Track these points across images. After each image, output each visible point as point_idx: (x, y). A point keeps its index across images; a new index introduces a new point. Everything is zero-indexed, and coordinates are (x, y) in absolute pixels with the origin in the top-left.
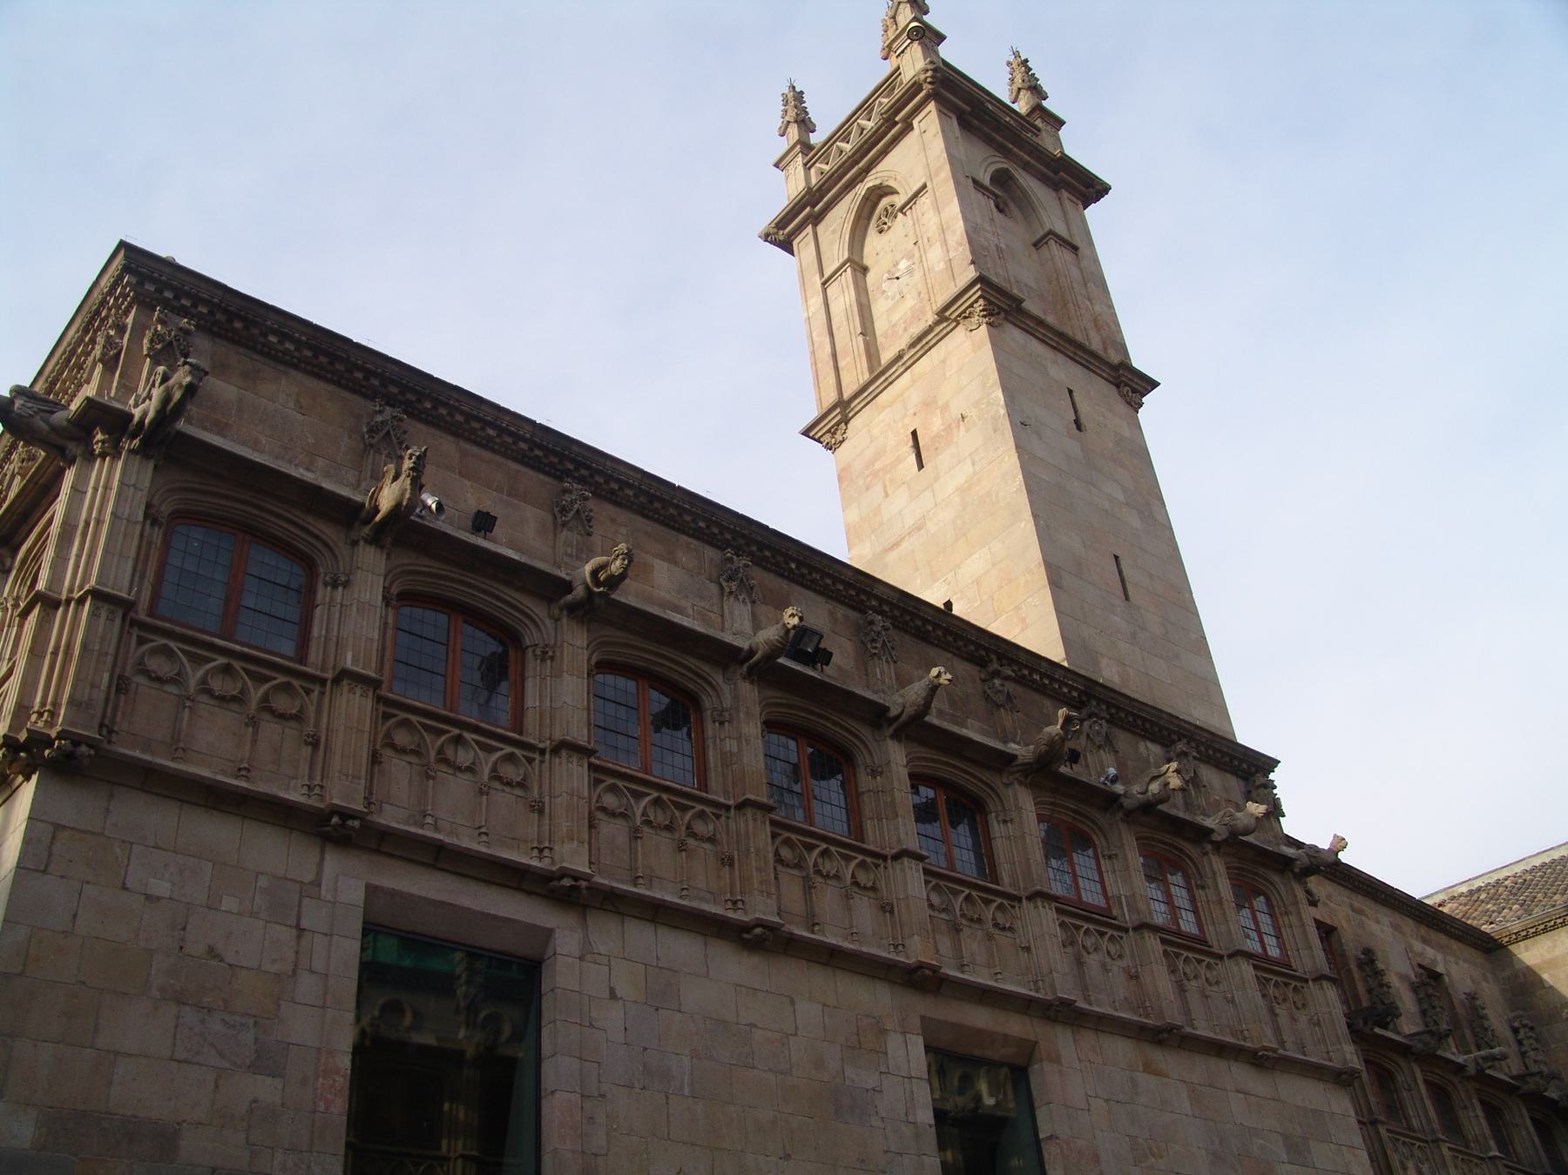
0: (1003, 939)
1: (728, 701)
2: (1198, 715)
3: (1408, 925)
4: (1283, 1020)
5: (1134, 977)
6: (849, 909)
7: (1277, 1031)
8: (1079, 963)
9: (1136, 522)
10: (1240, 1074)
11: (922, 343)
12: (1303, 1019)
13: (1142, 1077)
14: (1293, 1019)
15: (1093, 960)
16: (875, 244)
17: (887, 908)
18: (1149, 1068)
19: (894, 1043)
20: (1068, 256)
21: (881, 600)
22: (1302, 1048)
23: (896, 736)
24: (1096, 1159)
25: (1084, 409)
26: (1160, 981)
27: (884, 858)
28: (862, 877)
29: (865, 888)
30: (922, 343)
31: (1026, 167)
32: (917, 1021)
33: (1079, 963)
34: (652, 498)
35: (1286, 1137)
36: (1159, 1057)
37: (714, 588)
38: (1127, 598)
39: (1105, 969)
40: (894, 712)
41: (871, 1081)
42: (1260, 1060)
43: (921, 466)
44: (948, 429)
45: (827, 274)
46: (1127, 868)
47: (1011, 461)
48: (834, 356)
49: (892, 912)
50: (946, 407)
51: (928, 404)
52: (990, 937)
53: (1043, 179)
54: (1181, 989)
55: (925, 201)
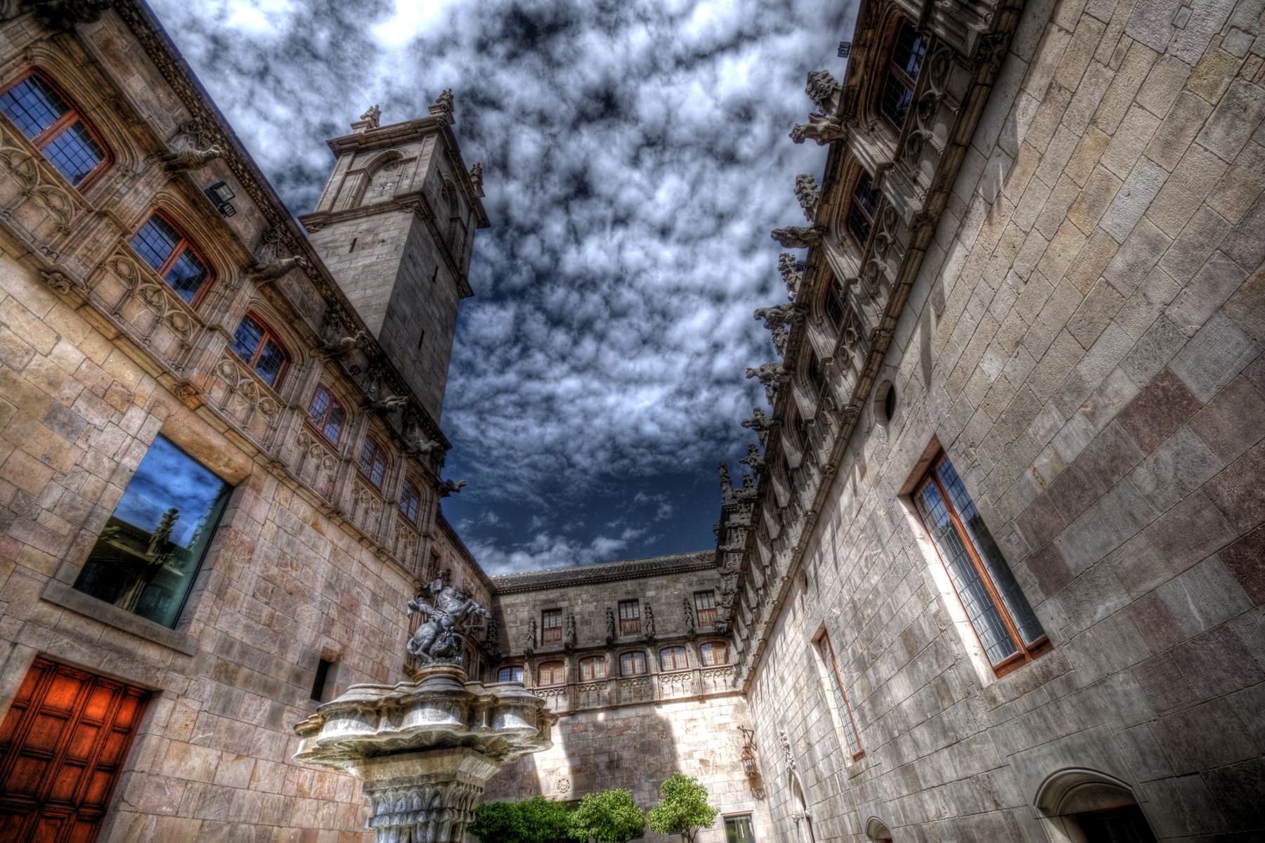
0: (261, 419)
1: (140, 168)
2: (429, 410)
3: (470, 571)
4: (401, 546)
5: (331, 480)
6: (154, 328)
7: (396, 548)
8: (304, 456)
9: (439, 329)
10: (366, 556)
11: (381, 209)
12: (409, 551)
13: (308, 528)
14: (405, 547)
15: (312, 462)
16: (381, 173)
17: (184, 347)
18: (315, 526)
19: (135, 417)
20: (462, 232)
21: (288, 229)
22: (403, 561)
23: (255, 280)
24: (252, 551)
25: (440, 277)
26: (347, 492)
27: (203, 326)
28: (179, 322)
29: (177, 329)
30: (381, 209)
31: (462, 192)
32: (163, 412)
33: (304, 456)
34: (159, 48)
35: (374, 594)
36: (324, 525)
37: (173, 126)
38: (420, 347)
39: (318, 468)
40: (260, 266)
41: (97, 421)
42: (380, 553)
43: (351, 251)
44: (373, 243)
45: (353, 168)
46: (357, 434)
47: (396, 263)
48: (335, 200)
49: (188, 350)
50: (377, 234)
51: (369, 231)
52: (252, 409)
53: (467, 202)
54: (356, 502)
55: (413, 164)
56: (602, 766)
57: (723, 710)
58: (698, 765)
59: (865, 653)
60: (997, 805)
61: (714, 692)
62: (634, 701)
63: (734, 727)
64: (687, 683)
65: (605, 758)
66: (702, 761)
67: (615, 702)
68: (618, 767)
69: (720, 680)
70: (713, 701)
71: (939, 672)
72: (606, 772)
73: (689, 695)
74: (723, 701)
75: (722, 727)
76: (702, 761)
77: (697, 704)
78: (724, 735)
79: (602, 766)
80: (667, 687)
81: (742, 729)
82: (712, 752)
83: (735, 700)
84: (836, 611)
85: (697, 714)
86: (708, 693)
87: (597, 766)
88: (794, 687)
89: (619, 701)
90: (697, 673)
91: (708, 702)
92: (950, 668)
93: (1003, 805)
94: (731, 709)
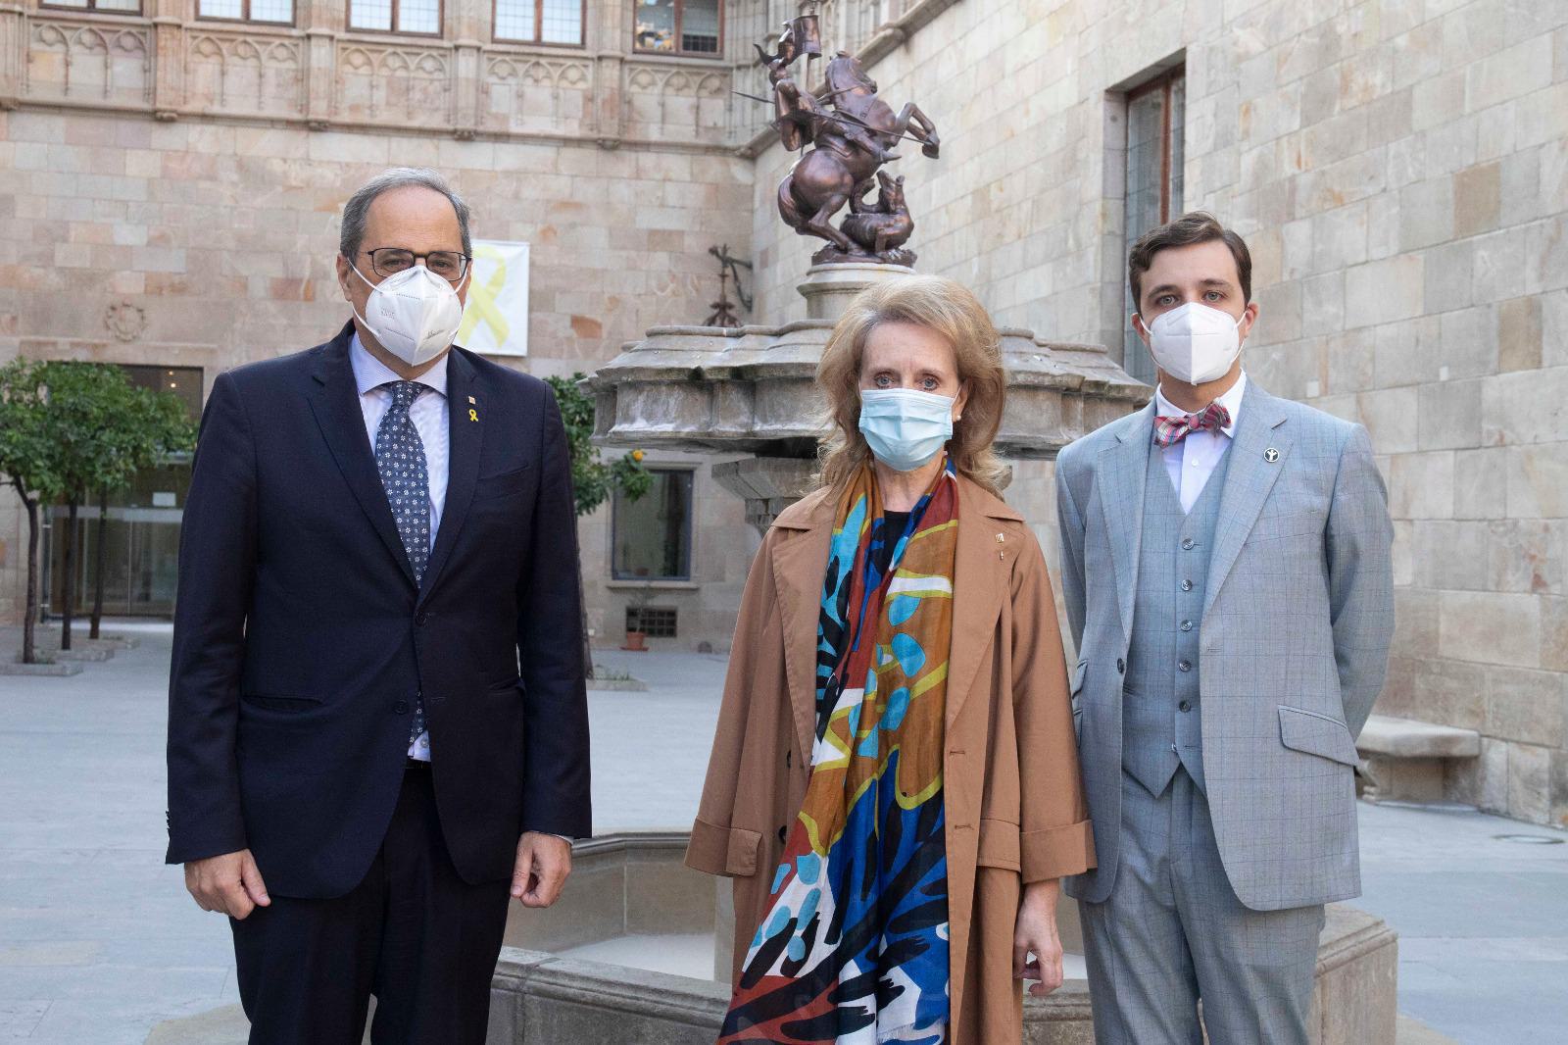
56: (259, 289)
57: (672, 194)
58: (565, 330)
59: (1304, 180)
60: (1538, 583)
61: (654, 135)
62: (383, 117)
63: (695, 245)
64: (574, 96)
65: (276, 271)
66: (577, 322)
67: (319, 111)
68: (309, 297)
69: (681, 104)
70: (647, 159)
71: (1533, 288)
72: (272, 307)
73: (574, 130)
74: (678, 165)
75: (659, 239)
76: (577, 322)
77: (590, 156)
78: (661, 259)
79: (259, 289)
80: (502, 96)
81: (720, 255)
82: (614, 301)
83: (714, 166)
84: (1250, 40)
85: (588, 192)
86: (636, 136)
87: (243, 285)
88: (981, 194)
89: (334, 109)
90: (611, 71)
91: (629, 160)
94: (695, 196)
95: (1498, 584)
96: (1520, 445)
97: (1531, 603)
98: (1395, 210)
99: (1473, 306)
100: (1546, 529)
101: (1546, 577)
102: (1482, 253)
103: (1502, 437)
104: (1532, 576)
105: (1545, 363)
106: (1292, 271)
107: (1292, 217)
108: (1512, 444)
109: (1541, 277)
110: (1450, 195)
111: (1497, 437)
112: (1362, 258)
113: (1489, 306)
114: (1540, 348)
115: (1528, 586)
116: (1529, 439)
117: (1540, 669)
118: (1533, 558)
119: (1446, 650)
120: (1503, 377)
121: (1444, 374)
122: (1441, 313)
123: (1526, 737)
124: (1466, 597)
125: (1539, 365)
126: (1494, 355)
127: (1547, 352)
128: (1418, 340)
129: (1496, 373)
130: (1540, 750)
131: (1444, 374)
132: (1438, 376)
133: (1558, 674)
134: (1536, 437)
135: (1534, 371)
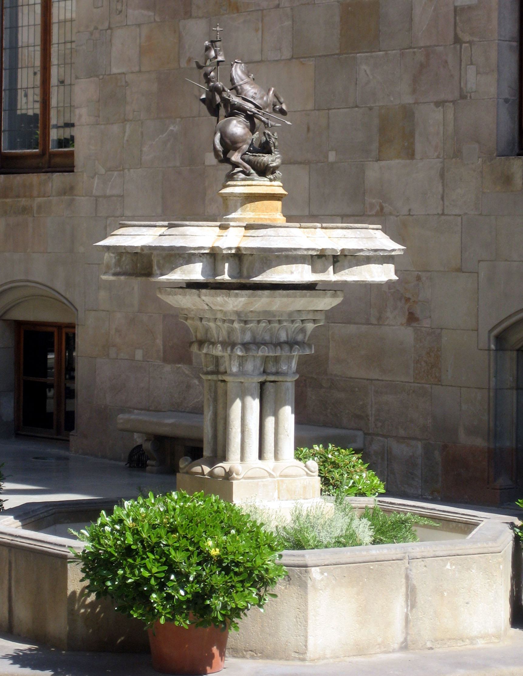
60: (412, 318)
71: (408, 99)
92: (439, 104)
93: (426, 323)
95: (379, 319)
96: (397, 216)
97: (406, 334)
98: (288, 23)
99: (357, 106)
100: (419, 278)
101: (418, 312)
102: (364, 67)
103: (382, 208)
104: (407, 313)
105: (418, 156)
106: (189, 60)
107: (188, 15)
108: (391, 214)
109: (414, 91)
110: (337, 19)
111: (378, 208)
112: (258, 58)
113: (371, 109)
114: (413, 143)
115: (404, 321)
116: (405, 211)
117: (414, 382)
118: (408, 300)
119: (335, 369)
120: (382, 163)
121: (332, 157)
122: (329, 109)
123: (402, 432)
124: (352, 329)
125: (411, 154)
126: (375, 146)
127: (418, 147)
128: (308, 129)
129: (378, 160)
130: (413, 443)
131: (332, 157)
132: (327, 157)
133: (427, 386)
134: (410, 210)
135: (408, 161)
